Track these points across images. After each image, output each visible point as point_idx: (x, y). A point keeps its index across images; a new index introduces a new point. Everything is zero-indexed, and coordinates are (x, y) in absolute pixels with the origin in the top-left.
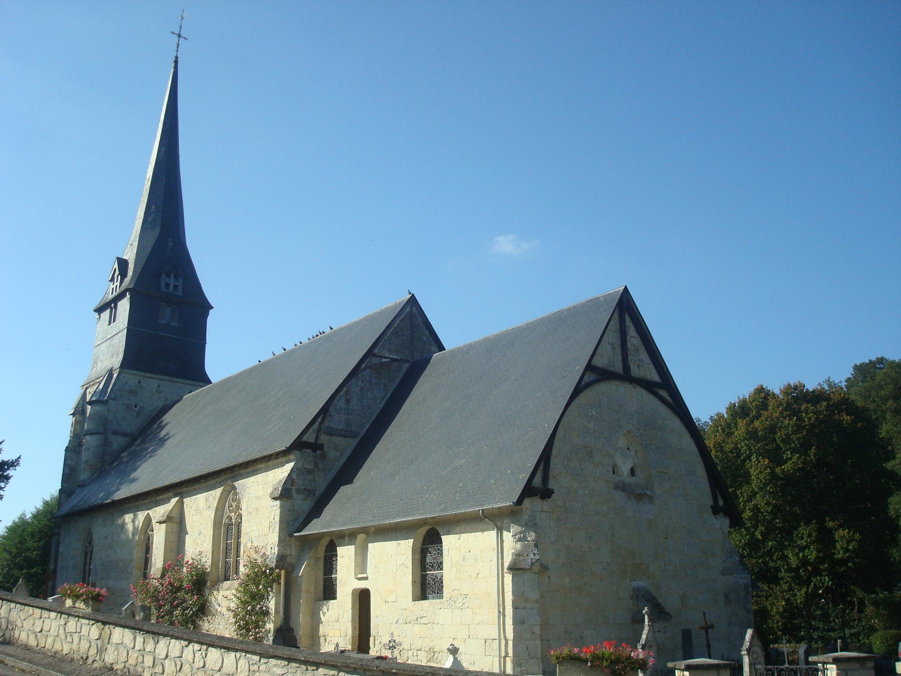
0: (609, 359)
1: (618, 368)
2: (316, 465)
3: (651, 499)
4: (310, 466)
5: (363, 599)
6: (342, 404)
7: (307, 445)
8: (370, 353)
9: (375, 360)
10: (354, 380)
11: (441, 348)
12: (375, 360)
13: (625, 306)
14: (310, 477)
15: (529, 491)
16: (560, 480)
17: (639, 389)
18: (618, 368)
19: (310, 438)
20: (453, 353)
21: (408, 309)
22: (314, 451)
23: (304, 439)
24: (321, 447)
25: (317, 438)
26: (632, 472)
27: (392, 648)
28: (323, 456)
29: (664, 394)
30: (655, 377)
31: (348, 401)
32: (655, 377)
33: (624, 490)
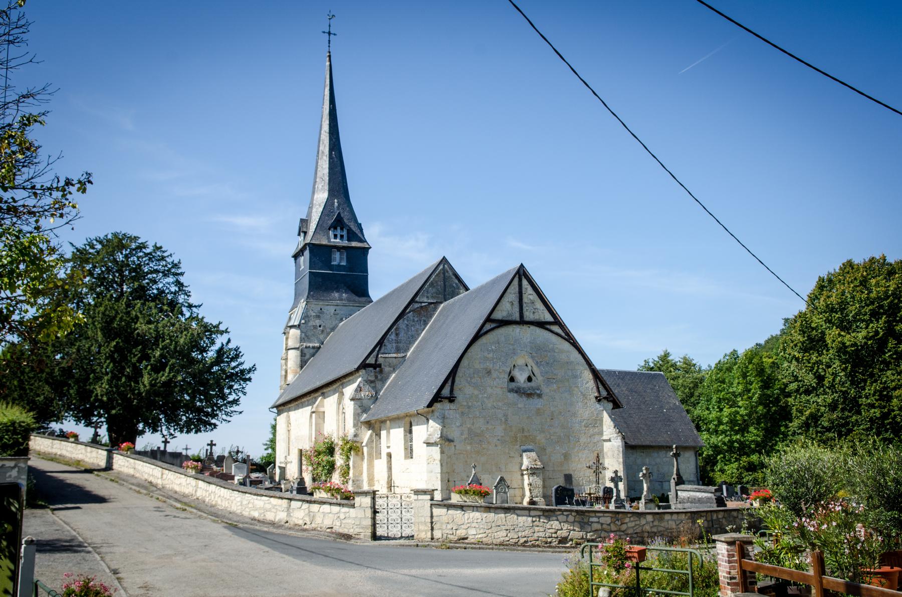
0: (507, 310)
1: (516, 317)
2: (376, 377)
3: (540, 396)
4: (372, 379)
5: (389, 455)
6: (393, 337)
7: (370, 365)
8: (413, 301)
9: (416, 306)
10: (401, 321)
11: (467, 289)
12: (416, 306)
13: (521, 273)
14: (373, 385)
15: (437, 398)
16: (464, 388)
17: (532, 327)
18: (516, 317)
19: (371, 360)
20: (480, 290)
21: (441, 267)
22: (375, 369)
23: (367, 362)
24: (380, 366)
25: (376, 360)
26: (530, 379)
27: (187, 449)
28: (381, 372)
29: (556, 328)
30: (549, 318)
31: (397, 335)
32: (549, 318)
33: (516, 392)
